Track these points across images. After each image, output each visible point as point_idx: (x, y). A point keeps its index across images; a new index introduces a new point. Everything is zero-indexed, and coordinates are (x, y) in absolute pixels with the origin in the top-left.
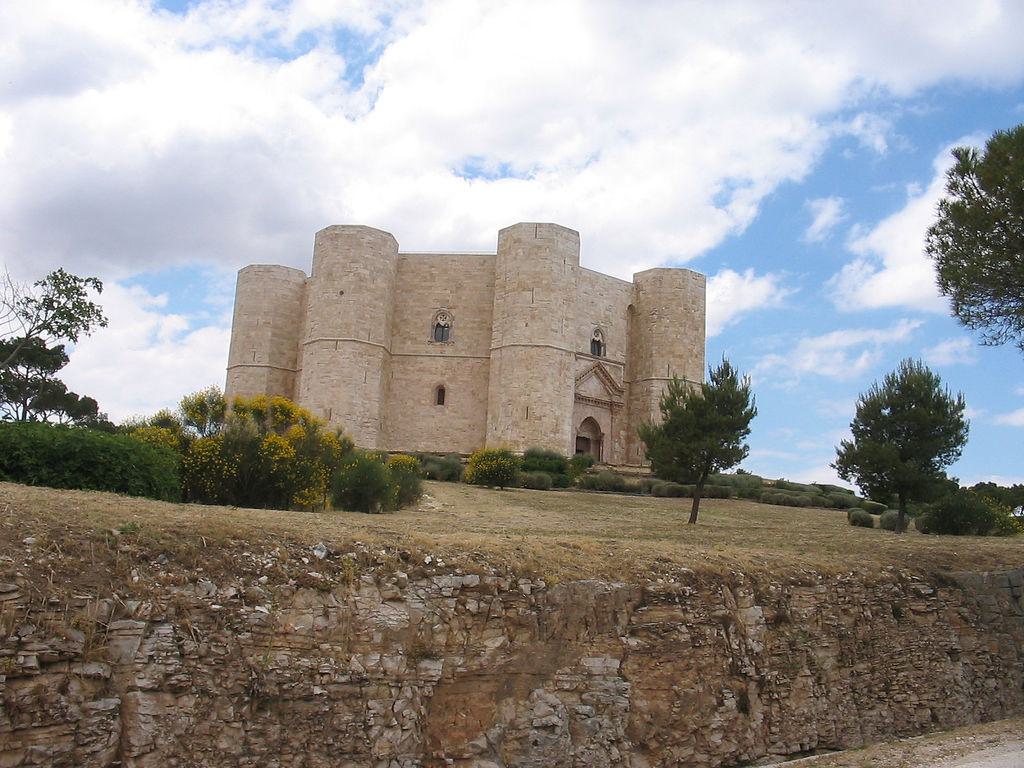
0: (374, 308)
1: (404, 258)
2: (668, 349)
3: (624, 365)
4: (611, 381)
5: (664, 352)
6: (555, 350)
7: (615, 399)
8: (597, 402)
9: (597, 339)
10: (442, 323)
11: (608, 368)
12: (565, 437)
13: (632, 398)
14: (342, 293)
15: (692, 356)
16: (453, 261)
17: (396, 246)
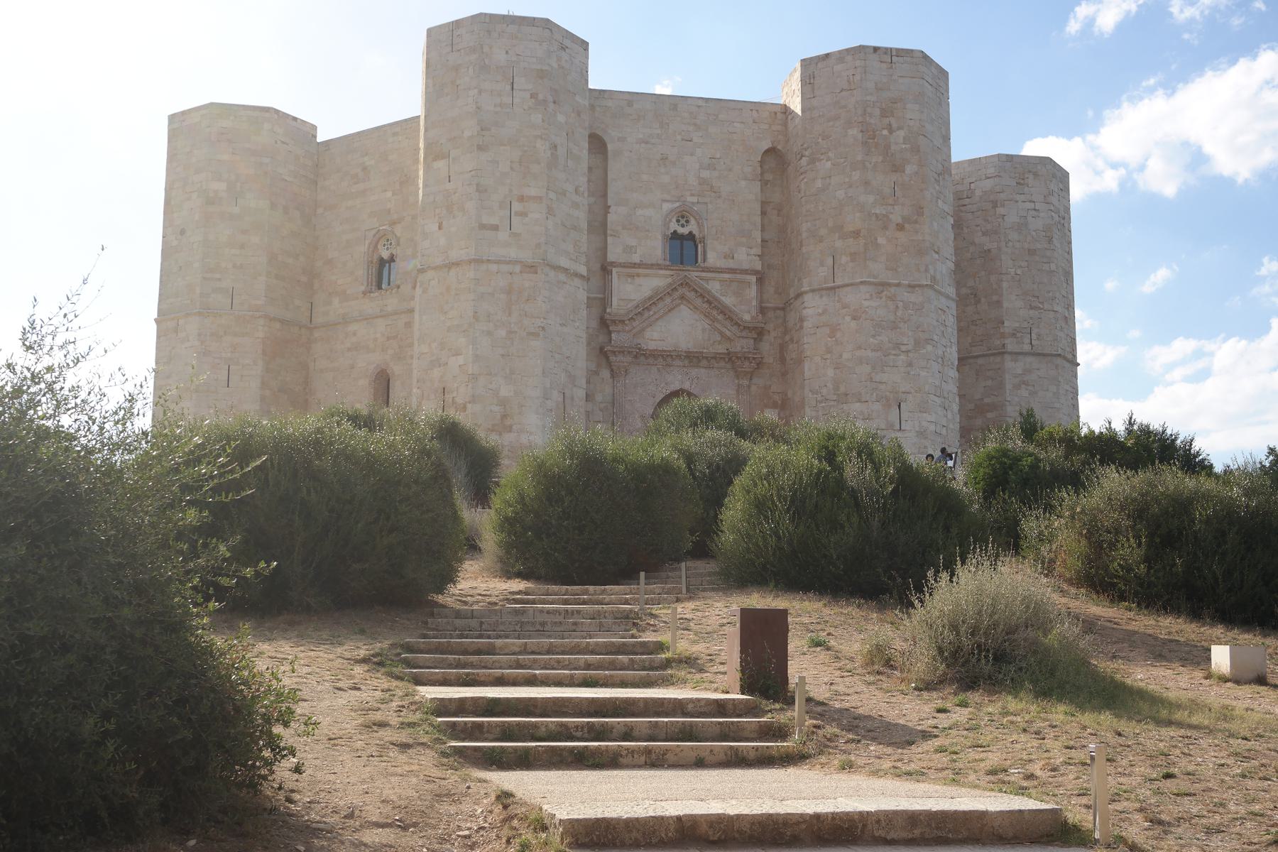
0: (242, 247)
1: (327, 144)
2: (830, 224)
3: (755, 272)
4: (725, 312)
5: (823, 232)
6: (494, 267)
7: (742, 345)
8: (693, 358)
9: (685, 231)
10: (385, 255)
11: (714, 287)
12: (524, 439)
13: (787, 338)
14: (183, 232)
15: (885, 228)
16: (395, 134)
17: (309, 131)
